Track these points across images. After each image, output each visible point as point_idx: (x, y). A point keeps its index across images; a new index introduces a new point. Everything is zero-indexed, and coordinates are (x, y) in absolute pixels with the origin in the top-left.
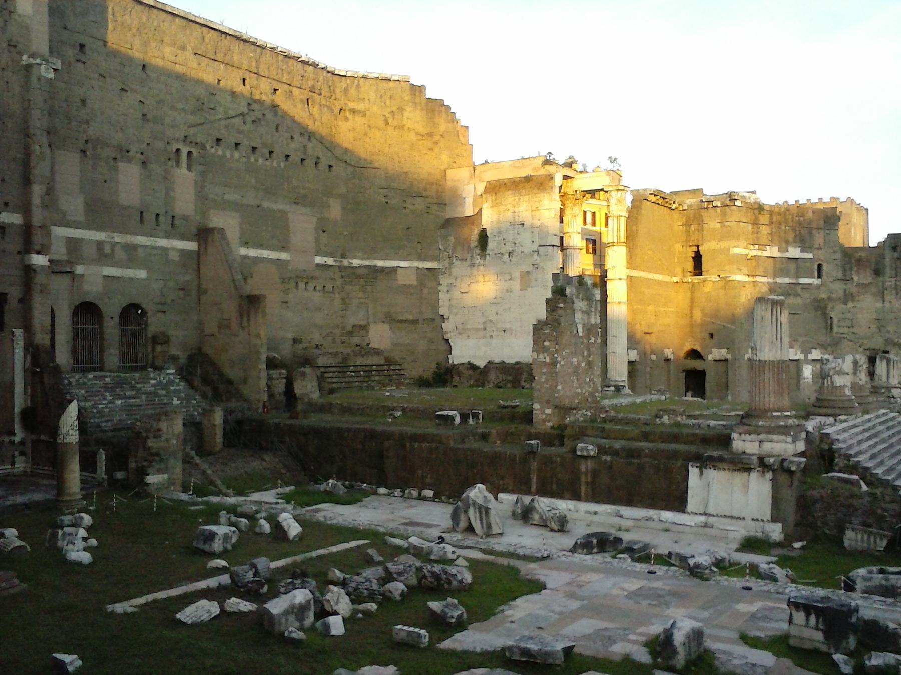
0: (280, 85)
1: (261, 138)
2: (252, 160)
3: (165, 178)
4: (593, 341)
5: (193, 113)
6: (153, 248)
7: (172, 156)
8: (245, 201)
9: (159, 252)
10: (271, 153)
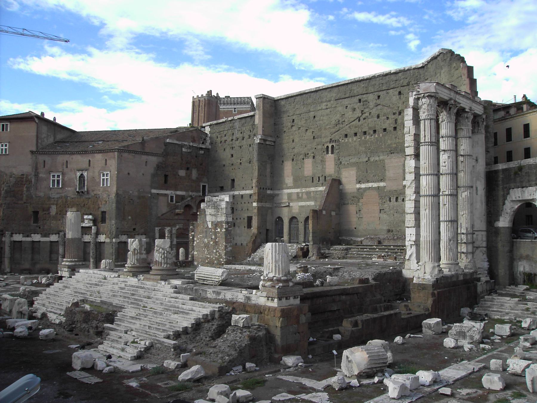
0: (380, 93)
1: (368, 125)
2: (363, 138)
3: (322, 161)
4: (219, 230)
5: (334, 127)
6: (316, 192)
7: (325, 150)
8: (361, 160)
9: (319, 193)
10: (375, 131)
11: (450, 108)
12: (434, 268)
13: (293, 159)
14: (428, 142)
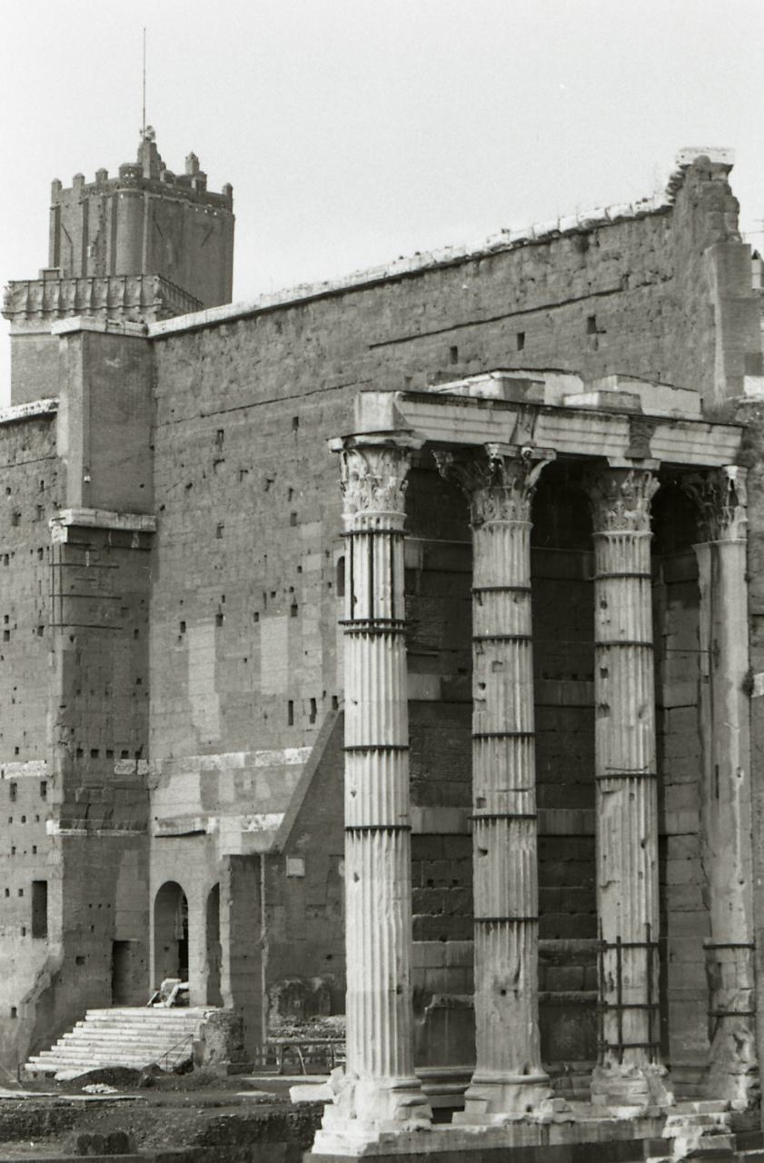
7: (334, 578)
11: (497, 476)
12: (383, 1093)
13: (220, 617)
14: (364, 622)
